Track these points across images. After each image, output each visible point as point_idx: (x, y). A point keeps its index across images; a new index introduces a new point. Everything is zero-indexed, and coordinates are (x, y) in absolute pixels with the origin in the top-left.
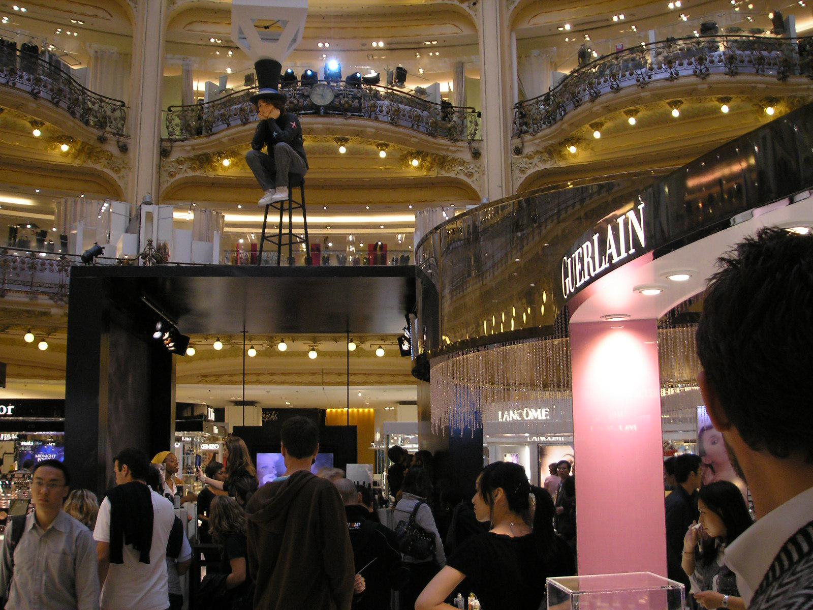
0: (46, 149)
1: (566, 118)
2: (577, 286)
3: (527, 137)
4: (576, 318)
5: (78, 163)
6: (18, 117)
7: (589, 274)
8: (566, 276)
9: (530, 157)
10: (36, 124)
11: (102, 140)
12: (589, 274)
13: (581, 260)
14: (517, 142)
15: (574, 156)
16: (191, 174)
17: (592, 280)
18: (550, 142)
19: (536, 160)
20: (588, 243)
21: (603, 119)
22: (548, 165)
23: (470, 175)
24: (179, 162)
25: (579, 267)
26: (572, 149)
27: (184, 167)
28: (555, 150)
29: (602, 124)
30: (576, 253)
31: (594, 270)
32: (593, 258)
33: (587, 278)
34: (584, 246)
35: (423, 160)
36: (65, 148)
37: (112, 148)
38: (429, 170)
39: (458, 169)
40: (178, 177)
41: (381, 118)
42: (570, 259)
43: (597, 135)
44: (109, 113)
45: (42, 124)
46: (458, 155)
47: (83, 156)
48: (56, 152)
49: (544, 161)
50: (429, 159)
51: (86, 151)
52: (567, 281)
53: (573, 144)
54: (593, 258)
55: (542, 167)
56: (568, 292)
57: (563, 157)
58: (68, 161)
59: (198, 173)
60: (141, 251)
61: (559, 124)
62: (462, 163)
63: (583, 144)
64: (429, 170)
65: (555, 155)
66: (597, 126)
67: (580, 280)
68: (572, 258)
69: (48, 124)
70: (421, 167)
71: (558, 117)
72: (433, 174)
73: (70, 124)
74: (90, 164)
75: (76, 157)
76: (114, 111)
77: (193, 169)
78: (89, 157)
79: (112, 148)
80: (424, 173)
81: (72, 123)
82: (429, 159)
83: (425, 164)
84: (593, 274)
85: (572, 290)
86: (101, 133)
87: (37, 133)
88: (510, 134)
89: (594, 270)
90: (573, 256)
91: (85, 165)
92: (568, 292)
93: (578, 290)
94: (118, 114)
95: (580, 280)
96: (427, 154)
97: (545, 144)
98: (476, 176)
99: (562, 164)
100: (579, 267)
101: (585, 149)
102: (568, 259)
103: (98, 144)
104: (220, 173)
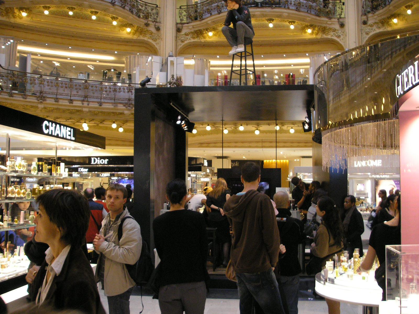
0: (119, 30)
1: (392, 3)
2: (405, 90)
3: (370, 15)
4: (403, 108)
5: (135, 37)
6: (105, 15)
7: (412, 83)
8: (398, 85)
9: (371, 26)
10: (114, 18)
11: (147, 25)
12: (412, 83)
13: (407, 76)
14: (364, 18)
15: (396, 24)
16: (192, 40)
17: (414, 86)
18: (383, 17)
19: (375, 27)
20: (411, 67)
21: (413, 3)
22: (381, 30)
23: (339, 37)
24: (186, 35)
25: (406, 80)
26: (395, 21)
27: (189, 37)
28: (385, 21)
29: (412, 6)
30: (404, 73)
31: (415, 81)
32: (414, 74)
33: (411, 85)
34: (409, 68)
35: (314, 29)
36: (129, 30)
37: (152, 29)
38: (317, 34)
39: (332, 33)
40: (186, 42)
41: (291, 7)
42: (401, 76)
43: (409, 12)
44: (150, 11)
45: (117, 18)
46: (333, 26)
47: (138, 34)
48: (124, 32)
49: (379, 28)
50: (317, 29)
51: (140, 31)
52: (398, 88)
53: (395, 18)
54: (414, 74)
55: (378, 31)
56: (399, 94)
57: (390, 25)
58: (130, 36)
59: (196, 40)
60: (168, 81)
61: (388, 6)
62: (334, 30)
63: (401, 18)
64: (317, 34)
65: (385, 25)
66: (409, 7)
67: (407, 87)
68: (402, 75)
69: (120, 18)
70: (313, 33)
71: (387, 3)
72: (319, 36)
73: (131, 17)
74: (141, 38)
75: (134, 34)
76: (152, 10)
77: (194, 38)
78: (141, 34)
79: (152, 29)
80: (314, 36)
81: (132, 17)
82: (317, 29)
83: (315, 31)
84: (414, 83)
85: (402, 93)
86: (146, 22)
87: (115, 23)
88: (360, 14)
89: (415, 81)
90: (402, 74)
91: (139, 38)
92: (399, 94)
93: (405, 92)
94: (154, 11)
95: (407, 87)
96: (316, 26)
97: (380, 18)
98: (342, 37)
99: (389, 29)
100: (406, 80)
101: (402, 20)
102: (399, 76)
103: (145, 27)
104: (208, 39)
